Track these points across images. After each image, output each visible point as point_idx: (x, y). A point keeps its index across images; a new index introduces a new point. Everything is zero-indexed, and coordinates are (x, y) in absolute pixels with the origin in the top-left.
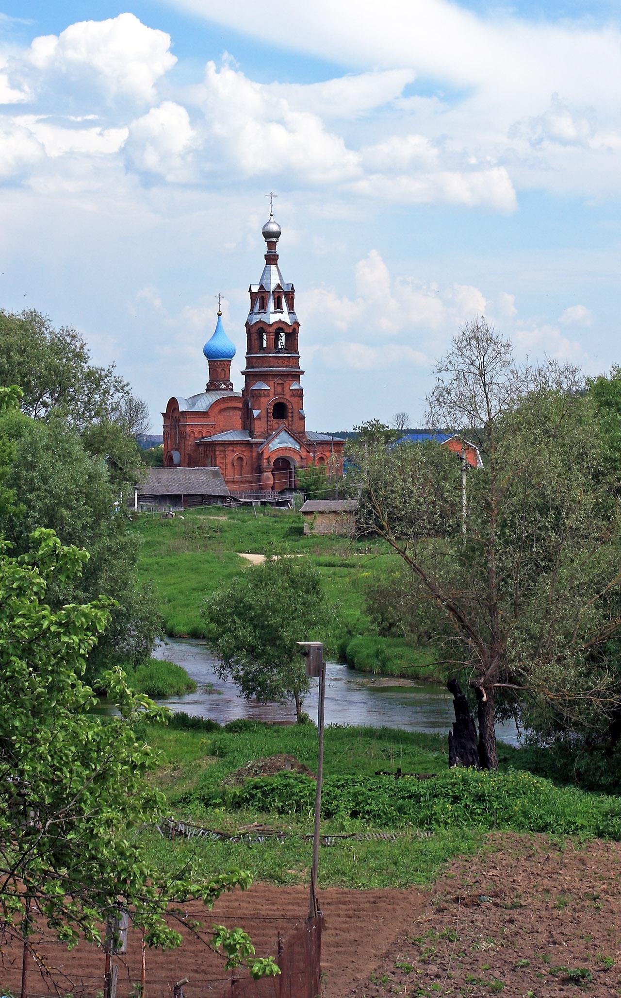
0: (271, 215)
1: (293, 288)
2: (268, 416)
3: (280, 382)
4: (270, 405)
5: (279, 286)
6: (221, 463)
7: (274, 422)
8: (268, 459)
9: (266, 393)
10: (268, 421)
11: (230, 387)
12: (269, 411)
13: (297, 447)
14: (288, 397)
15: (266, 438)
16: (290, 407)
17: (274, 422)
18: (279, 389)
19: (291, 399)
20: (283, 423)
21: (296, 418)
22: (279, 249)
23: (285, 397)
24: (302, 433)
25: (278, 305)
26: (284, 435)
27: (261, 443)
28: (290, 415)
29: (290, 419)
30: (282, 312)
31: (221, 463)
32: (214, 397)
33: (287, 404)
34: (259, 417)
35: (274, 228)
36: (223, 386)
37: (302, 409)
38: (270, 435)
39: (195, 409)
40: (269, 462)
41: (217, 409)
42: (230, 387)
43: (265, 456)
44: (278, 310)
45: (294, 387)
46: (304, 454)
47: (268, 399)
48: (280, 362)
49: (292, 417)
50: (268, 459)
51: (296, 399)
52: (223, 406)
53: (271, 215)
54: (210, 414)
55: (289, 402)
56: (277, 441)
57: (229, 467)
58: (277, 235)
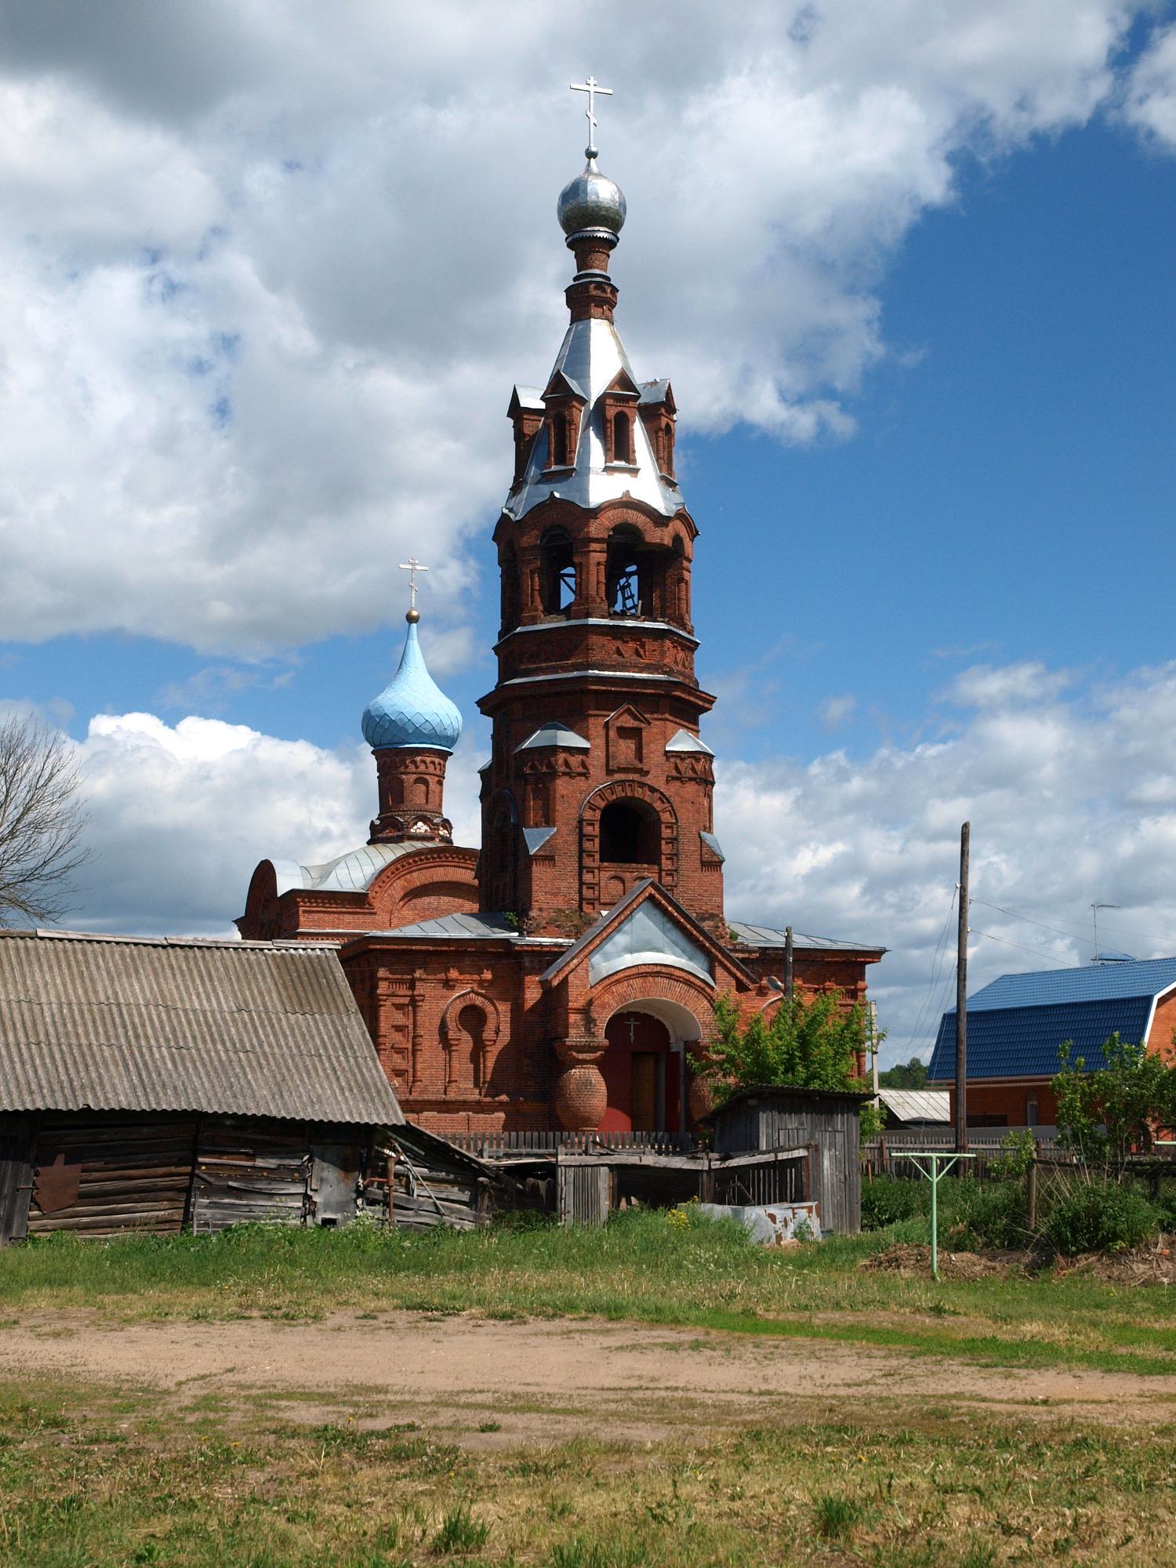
0: (591, 155)
1: (669, 394)
2: (581, 851)
3: (628, 722)
4: (593, 808)
5: (624, 380)
6: (399, 1029)
7: (605, 877)
8: (586, 1011)
9: (575, 761)
10: (581, 868)
11: (443, 832)
12: (588, 830)
13: (696, 967)
14: (656, 779)
15: (577, 933)
16: (666, 817)
17: (605, 875)
18: (625, 750)
19: (670, 790)
20: (641, 879)
21: (689, 863)
22: (616, 266)
23: (649, 780)
24: (712, 916)
25: (620, 449)
26: (644, 923)
27: (551, 955)
28: (665, 848)
29: (666, 864)
30: (634, 472)
31: (399, 1029)
32: (389, 854)
33: (658, 806)
34: (548, 858)
35: (602, 191)
36: (421, 828)
37: (709, 829)
38: (590, 923)
39: (331, 885)
40: (589, 1022)
41: (399, 887)
42: (443, 832)
43: (576, 998)
44: (616, 463)
45: (682, 742)
46: (724, 987)
47: (581, 782)
48: (628, 649)
49: (674, 856)
50: (586, 1011)
51: (691, 788)
52: (418, 878)
53: (591, 155)
54: (377, 904)
55: (664, 798)
56: (620, 939)
57: (429, 1041)
58: (613, 220)
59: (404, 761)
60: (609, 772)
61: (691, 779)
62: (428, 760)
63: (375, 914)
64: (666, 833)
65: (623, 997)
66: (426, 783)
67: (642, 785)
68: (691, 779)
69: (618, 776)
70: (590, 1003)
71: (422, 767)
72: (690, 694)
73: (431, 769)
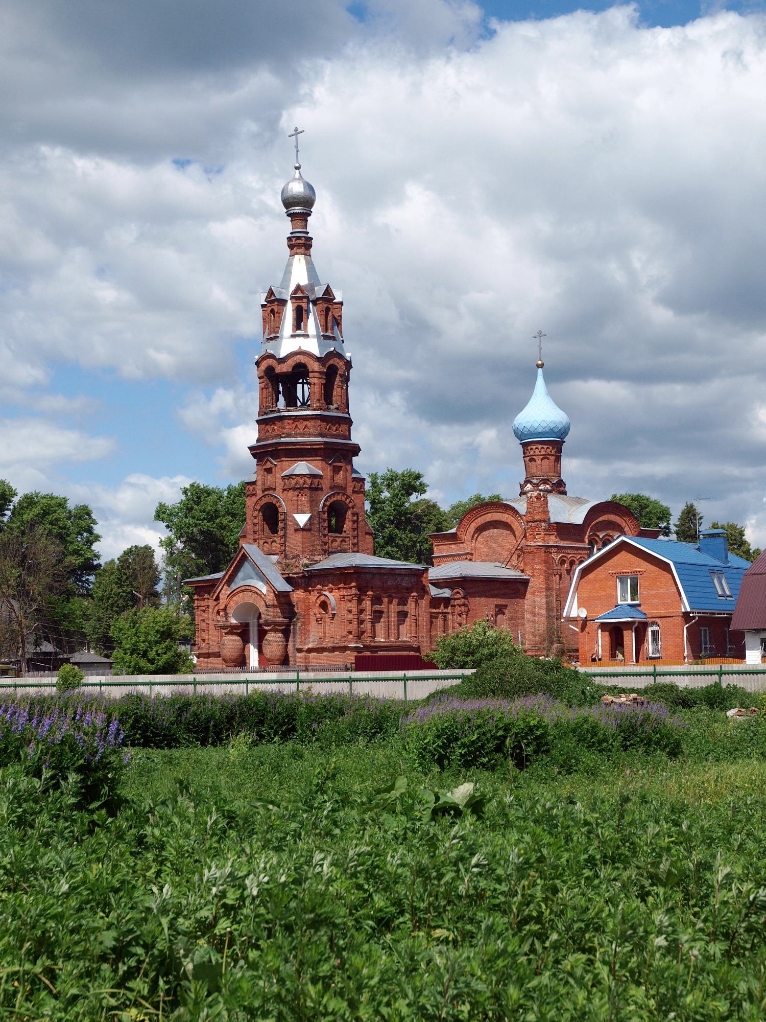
3: (268, 465)
28: (281, 525)
49: (285, 528)
59: (527, 450)
60: (263, 491)
61: (290, 489)
62: (534, 447)
63: (463, 543)
64: (281, 517)
65: (237, 603)
66: (534, 460)
67: (272, 496)
68: (290, 489)
69: (266, 493)
70: (226, 606)
71: (532, 452)
72: (295, 445)
73: (537, 452)
